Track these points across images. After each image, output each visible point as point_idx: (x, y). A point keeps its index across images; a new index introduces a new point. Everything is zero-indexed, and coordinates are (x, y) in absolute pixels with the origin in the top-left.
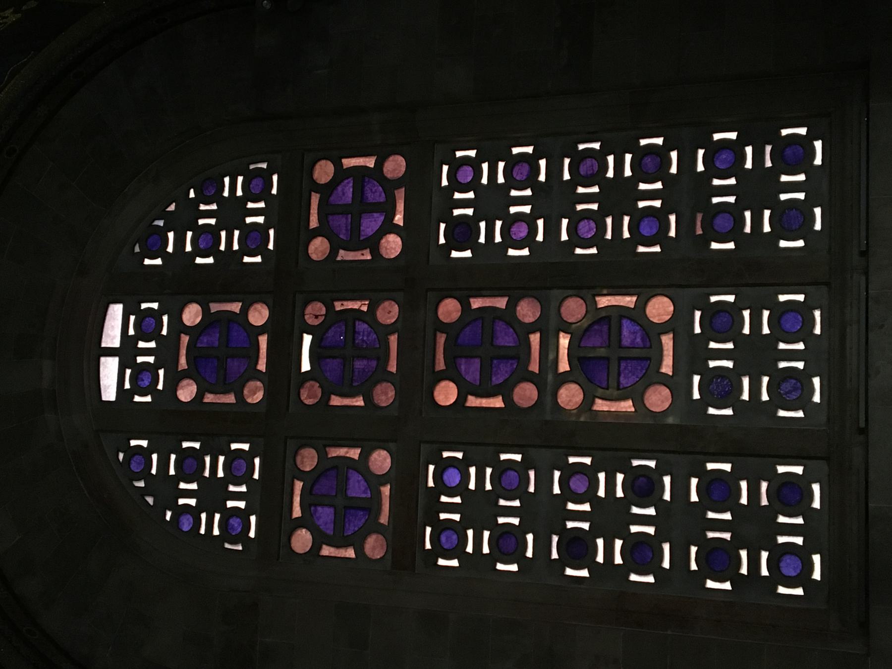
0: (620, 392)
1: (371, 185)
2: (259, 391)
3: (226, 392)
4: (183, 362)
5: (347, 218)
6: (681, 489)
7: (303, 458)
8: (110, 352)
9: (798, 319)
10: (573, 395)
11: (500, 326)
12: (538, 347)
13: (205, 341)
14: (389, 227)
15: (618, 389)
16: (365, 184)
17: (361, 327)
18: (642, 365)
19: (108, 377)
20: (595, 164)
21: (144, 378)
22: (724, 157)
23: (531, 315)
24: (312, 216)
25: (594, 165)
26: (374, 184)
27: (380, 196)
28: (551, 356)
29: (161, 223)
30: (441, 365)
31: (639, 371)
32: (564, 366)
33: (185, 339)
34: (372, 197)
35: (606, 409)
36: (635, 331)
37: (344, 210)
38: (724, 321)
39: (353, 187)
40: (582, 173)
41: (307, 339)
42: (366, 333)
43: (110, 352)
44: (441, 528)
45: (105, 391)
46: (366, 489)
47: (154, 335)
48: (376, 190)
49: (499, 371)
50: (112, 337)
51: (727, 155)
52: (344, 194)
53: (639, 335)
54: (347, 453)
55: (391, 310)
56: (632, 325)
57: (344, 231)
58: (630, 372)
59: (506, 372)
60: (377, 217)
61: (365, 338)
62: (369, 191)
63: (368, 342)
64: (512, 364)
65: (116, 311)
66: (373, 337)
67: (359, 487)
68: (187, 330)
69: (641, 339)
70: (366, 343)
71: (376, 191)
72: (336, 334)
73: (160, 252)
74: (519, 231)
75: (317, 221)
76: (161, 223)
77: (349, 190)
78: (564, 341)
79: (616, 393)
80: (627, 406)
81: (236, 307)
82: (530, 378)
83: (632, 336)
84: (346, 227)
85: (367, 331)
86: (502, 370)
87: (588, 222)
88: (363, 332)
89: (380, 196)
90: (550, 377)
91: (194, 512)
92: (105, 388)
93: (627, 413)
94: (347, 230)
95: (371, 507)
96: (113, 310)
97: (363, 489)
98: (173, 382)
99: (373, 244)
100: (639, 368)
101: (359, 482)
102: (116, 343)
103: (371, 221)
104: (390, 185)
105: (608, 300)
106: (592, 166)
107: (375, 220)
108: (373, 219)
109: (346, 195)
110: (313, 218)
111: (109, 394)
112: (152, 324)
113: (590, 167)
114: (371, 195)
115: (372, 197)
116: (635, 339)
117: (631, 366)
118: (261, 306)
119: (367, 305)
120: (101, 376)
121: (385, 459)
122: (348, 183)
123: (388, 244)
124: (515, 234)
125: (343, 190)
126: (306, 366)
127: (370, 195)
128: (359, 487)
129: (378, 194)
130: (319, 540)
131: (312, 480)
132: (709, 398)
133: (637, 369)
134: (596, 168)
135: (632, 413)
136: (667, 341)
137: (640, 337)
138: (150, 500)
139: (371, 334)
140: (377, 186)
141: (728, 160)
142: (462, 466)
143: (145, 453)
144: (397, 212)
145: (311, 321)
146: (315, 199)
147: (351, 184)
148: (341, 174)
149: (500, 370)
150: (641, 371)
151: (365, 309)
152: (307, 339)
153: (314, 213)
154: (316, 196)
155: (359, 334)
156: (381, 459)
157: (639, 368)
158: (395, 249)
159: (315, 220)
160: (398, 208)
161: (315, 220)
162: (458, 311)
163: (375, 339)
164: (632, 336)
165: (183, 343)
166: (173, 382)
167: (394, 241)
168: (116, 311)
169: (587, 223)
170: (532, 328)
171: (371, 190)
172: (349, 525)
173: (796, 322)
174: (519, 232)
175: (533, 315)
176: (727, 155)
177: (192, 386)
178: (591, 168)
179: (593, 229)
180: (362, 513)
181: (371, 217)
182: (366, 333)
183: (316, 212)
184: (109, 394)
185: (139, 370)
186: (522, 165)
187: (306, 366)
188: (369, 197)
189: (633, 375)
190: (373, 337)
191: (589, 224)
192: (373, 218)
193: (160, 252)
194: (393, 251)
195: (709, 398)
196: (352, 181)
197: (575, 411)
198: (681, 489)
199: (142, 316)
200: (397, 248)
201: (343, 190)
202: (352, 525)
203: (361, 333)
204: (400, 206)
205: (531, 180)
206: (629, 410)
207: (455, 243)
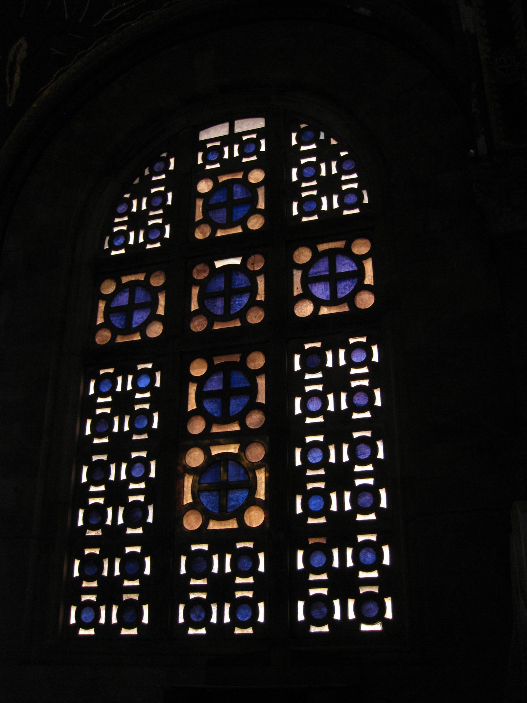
0: (196, 492)
1: (351, 284)
2: (203, 235)
3: (203, 212)
4: (223, 179)
5: (325, 271)
6: (134, 540)
7: (158, 276)
8: (232, 128)
9: (245, 617)
10: (195, 460)
11: (245, 400)
12: (229, 430)
13: (238, 190)
14: (318, 303)
15: (198, 491)
16: (351, 280)
17: (245, 299)
18: (215, 507)
19: (215, 131)
20: (366, 456)
21: (213, 155)
22: (369, 555)
23: (251, 422)
24: (327, 245)
25: (364, 455)
26: (351, 286)
27: (342, 293)
28: (221, 440)
29: (322, 136)
30: (217, 361)
31: (210, 506)
32: (215, 451)
33: (240, 176)
34: (341, 287)
35: (186, 484)
36: (239, 500)
37: (332, 266)
38: (245, 564)
39: (349, 272)
40: (359, 446)
41: (237, 261)
42: (240, 302)
43: (232, 128)
44: (112, 378)
45: (206, 132)
46: (138, 323)
47: (243, 153)
48: (346, 289)
49: (212, 404)
50: (241, 126)
51: (371, 557)
52: (344, 265)
53: (236, 503)
54: (161, 305)
55: (257, 317)
56: (243, 497)
57: (315, 271)
58: (210, 499)
59: (212, 409)
60: (325, 294)
61: (237, 302)
62: (346, 284)
63: (234, 305)
64: (217, 412)
65: (260, 123)
66: (238, 308)
67: (139, 318)
68: (246, 176)
69: (233, 505)
70: (234, 304)
71: (345, 289)
72: (241, 281)
73: (301, 142)
74: (314, 404)
75: (323, 250)
76: (322, 136)
77: (346, 269)
78: (233, 449)
79: (196, 490)
80: (188, 499)
81: (261, 205)
82: (208, 427)
83: (235, 498)
84: (319, 272)
85: (242, 303)
86: (213, 406)
87: (320, 456)
88: (241, 300)
89: (342, 293)
90: (207, 441)
91: (128, 212)
92: (205, 132)
93: (182, 499)
94: (316, 273)
95: (128, 330)
96: (260, 122)
97: (138, 321)
98: (213, 175)
99: (307, 295)
100: (213, 506)
101: (142, 317)
102: (237, 130)
103: (322, 290)
104: (350, 299)
105: (261, 477)
106: (364, 454)
107: (323, 293)
108: (324, 291)
109: (343, 267)
110: (326, 246)
111: (204, 136)
112: (250, 150)
113: (363, 452)
114: (342, 286)
115: (341, 287)
116: (234, 501)
117: (214, 499)
118: (261, 223)
119: (260, 299)
120: (216, 126)
121: (156, 332)
122: (352, 267)
123: (305, 306)
124: (312, 401)
125: (347, 264)
126: (219, 264)
127: (343, 285)
128: (139, 318)
129: (344, 291)
130: (109, 298)
131: (145, 285)
132: (193, 557)
133: (212, 504)
134: (362, 457)
135: (182, 503)
136: (232, 524)
137: (234, 504)
138: (137, 181)
139: (239, 307)
140: (349, 290)
141: (366, 559)
142: (151, 388)
143: (165, 170)
144: (329, 308)
145: (250, 260)
146: (339, 244)
147: (351, 269)
148: (359, 260)
149: (213, 405)
150: (210, 507)
151: (258, 298)
152: (237, 261)
153: (329, 246)
154: (342, 245)
155: (240, 298)
156: (156, 330)
157: (213, 506)
158: (301, 312)
159: (323, 248)
160: (333, 308)
161: (323, 248)
162: (255, 367)
163: (237, 310)
164: (235, 498)
165: (237, 175)
166: (213, 175)
167: (307, 310)
168: (260, 123)
169: (319, 455)
170: (243, 424)
171: (346, 285)
172: (116, 317)
173: (243, 616)
174: (313, 404)
175: (251, 423)
176: (371, 557)
177: (208, 188)
178: (362, 453)
179: (314, 460)
180: (123, 323)
181: (325, 289)
182: (240, 302)
183: (330, 247)
184: (204, 136)
185: (219, 150)
186: (365, 399)
187: (219, 264)
188: (342, 285)
189: (209, 502)
190: (238, 308)
191: (318, 457)
192: (325, 291)
193: (301, 142)
194: (300, 311)
195: (193, 557)
196: (353, 270)
197: (184, 463)
198: (134, 540)
199: (256, 142)
200: (302, 313)
201: (347, 264)
202: (116, 318)
203: (240, 299)
204: (334, 310)
205: (353, 407)
206: (185, 500)
207: (305, 355)
